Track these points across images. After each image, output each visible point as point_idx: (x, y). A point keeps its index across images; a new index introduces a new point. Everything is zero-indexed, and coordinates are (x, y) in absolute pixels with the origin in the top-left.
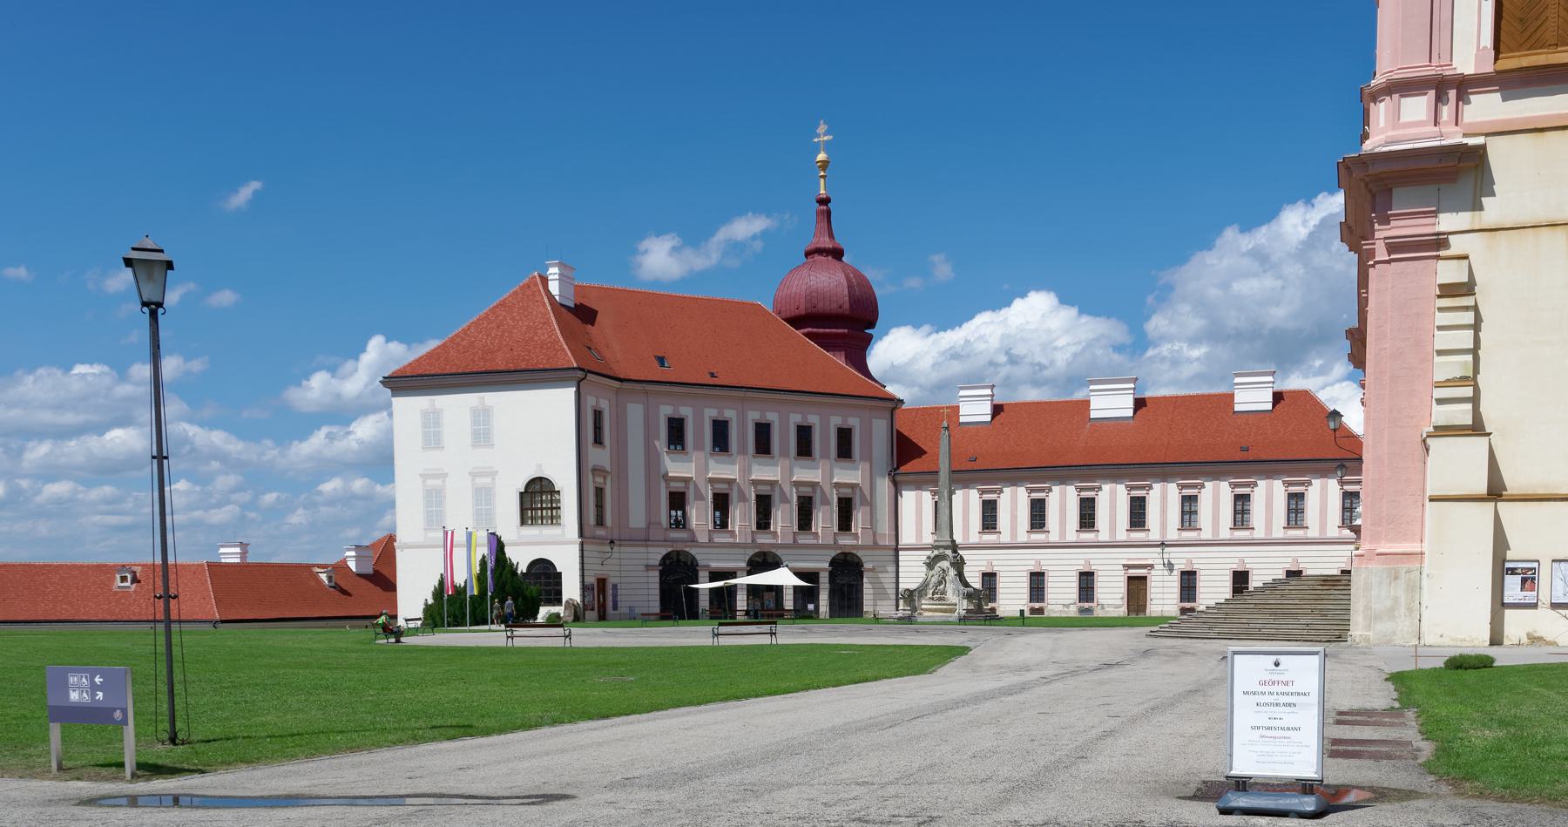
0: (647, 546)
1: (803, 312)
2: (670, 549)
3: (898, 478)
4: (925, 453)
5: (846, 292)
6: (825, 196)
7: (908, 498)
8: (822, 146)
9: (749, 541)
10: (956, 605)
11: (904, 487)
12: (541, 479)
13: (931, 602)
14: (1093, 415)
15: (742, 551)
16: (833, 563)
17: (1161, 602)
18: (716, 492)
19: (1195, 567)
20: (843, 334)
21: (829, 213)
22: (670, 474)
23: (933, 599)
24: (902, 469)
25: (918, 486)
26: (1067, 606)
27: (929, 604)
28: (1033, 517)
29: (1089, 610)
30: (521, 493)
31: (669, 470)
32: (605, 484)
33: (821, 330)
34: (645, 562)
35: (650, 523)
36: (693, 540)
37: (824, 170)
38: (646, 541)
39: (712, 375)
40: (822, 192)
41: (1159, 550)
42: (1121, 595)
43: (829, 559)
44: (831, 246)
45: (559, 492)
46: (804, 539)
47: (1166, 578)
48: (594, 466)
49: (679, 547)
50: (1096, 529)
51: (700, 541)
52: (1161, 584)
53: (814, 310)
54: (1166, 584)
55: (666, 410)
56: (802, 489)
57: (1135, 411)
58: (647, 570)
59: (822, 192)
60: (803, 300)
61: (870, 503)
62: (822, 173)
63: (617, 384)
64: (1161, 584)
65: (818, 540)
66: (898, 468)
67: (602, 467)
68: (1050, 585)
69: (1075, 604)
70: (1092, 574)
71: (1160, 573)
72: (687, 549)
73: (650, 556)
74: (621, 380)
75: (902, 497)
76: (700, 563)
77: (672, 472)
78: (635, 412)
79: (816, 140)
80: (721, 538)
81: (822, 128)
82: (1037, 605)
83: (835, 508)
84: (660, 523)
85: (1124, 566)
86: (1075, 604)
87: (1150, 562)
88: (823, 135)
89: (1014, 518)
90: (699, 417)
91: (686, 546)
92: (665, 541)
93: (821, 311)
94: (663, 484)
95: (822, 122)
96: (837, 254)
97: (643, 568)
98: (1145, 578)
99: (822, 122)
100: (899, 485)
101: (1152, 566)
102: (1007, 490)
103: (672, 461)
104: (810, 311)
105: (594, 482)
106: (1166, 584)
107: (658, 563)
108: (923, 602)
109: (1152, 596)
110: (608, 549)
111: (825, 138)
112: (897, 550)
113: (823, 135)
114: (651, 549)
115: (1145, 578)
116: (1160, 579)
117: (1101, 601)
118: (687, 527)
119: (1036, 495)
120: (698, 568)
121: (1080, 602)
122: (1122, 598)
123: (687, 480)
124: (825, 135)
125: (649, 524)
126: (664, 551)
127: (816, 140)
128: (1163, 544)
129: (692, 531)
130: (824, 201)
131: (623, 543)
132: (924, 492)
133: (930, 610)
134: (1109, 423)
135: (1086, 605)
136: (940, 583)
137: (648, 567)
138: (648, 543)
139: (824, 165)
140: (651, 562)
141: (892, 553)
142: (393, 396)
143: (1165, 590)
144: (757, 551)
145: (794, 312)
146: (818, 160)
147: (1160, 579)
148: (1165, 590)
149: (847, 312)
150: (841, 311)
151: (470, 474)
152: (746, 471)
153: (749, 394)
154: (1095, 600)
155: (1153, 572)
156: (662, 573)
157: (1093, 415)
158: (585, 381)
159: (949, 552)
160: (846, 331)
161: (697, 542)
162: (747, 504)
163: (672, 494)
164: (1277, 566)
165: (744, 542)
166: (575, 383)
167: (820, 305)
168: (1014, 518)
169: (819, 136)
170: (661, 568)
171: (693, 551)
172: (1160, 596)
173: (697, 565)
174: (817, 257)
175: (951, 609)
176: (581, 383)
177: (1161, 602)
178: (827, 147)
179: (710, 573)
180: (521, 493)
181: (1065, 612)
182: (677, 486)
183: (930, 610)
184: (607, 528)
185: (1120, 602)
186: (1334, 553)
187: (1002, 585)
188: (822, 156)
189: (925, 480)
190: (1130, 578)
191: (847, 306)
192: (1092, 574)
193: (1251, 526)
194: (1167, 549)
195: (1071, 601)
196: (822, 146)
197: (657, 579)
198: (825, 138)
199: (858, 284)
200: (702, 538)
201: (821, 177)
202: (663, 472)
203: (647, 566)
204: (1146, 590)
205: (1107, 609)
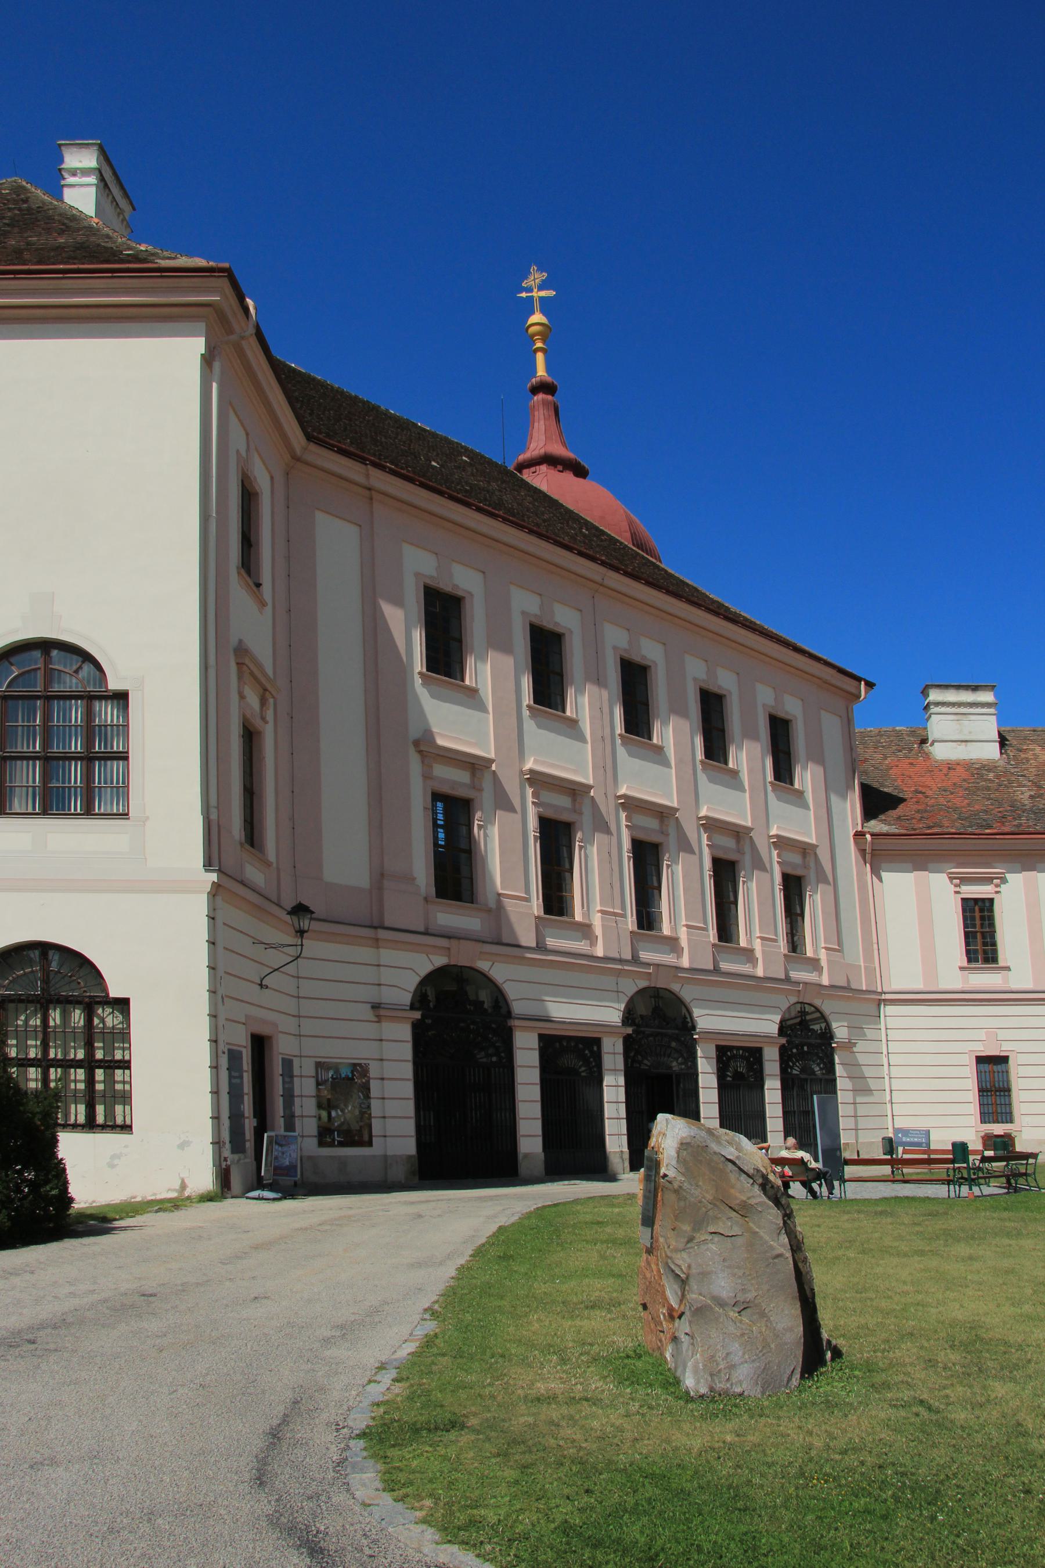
0: (376, 943)
2: (440, 961)
8: (537, 305)
9: (627, 955)
31: (435, 730)
34: (370, 994)
37: (544, 341)
49: (464, 956)
58: (379, 1019)
59: (541, 371)
62: (539, 345)
72: (483, 965)
73: (387, 976)
76: (517, 1008)
77: (442, 736)
79: (524, 295)
81: (536, 277)
92: (426, 933)
107: (407, 999)
111: (543, 294)
114: (387, 955)
123: (475, 766)
124: (541, 288)
125: (380, 877)
126: (425, 964)
127: (524, 295)
138: (382, 934)
140: (389, 996)
152: (610, 770)
156: (418, 1030)
169: (529, 290)
170: (417, 1015)
171: (500, 972)
173: (509, 1014)
179: (542, 1037)
182: (453, 778)
196: (537, 305)
197: (406, 1051)
198: (543, 294)
200: (527, 937)
202: (414, 733)
203: (376, 1007)
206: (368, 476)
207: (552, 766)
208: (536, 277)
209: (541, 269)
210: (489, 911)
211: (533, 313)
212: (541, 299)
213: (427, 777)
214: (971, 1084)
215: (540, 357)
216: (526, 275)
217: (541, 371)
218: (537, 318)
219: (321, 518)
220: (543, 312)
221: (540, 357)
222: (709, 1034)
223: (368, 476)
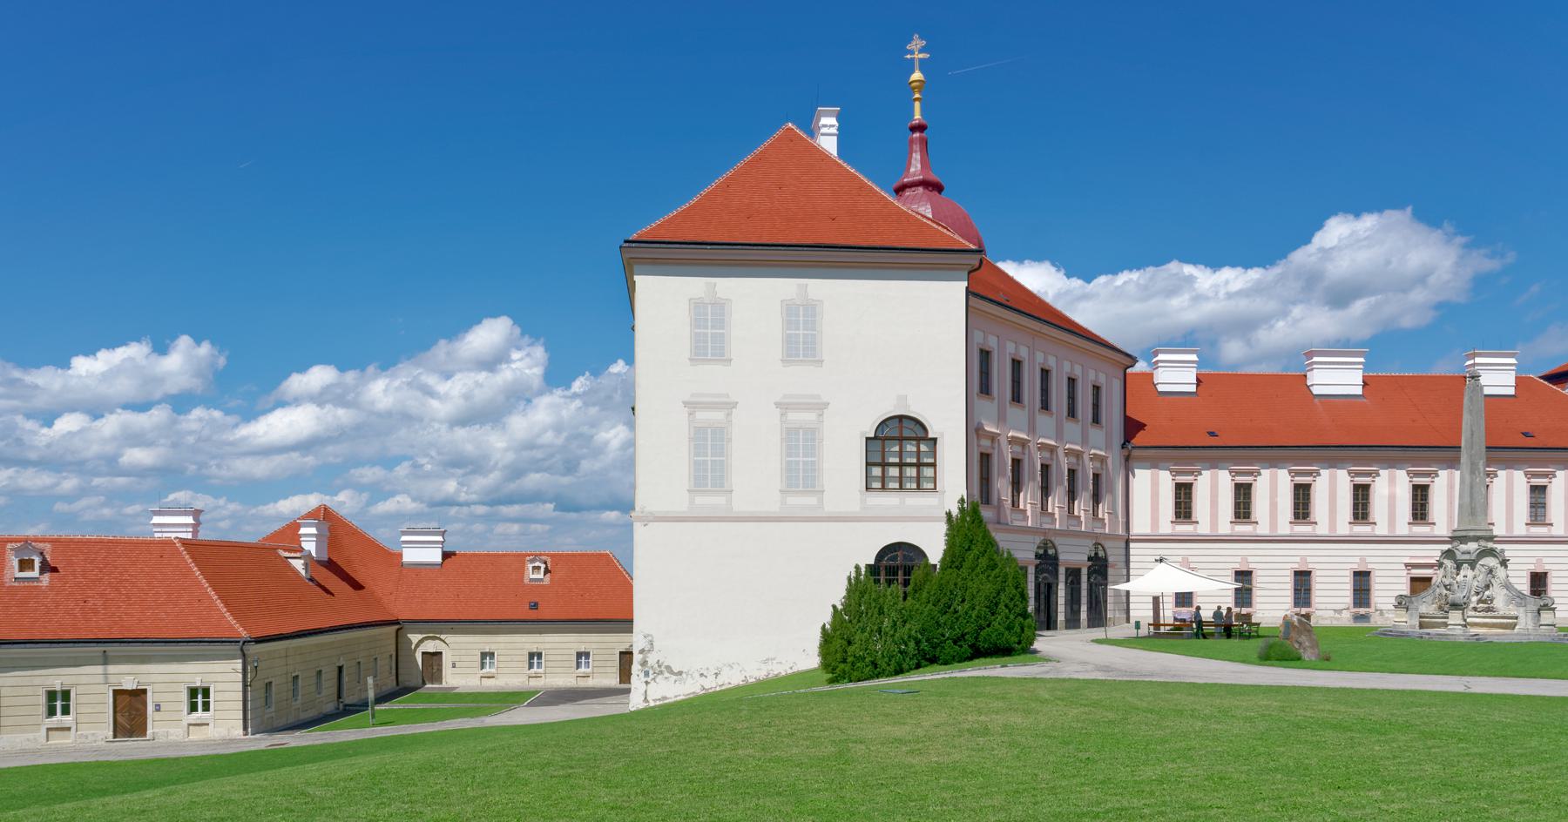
4: (1145, 425)
6: (917, 122)
7: (1142, 479)
8: (917, 64)
10: (1517, 618)
12: (901, 418)
18: (1015, 457)
19: (1251, 566)
23: (1475, 609)
24: (1136, 441)
25: (1154, 464)
26: (1339, 611)
29: (1365, 617)
30: (867, 439)
37: (920, 92)
45: (935, 440)
50: (1194, 519)
59: (917, 116)
62: (917, 96)
69: (1348, 609)
70: (1367, 574)
79: (909, 56)
81: (916, 44)
82: (1304, 611)
85: (1407, 565)
86: (1348, 609)
88: (916, 49)
89: (1274, 506)
95: (916, 36)
99: (916, 36)
100: (1131, 463)
102: (1266, 473)
111: (921, 56)
112: (1127, 542)
113: (916, 49)
117: (1380, 606)
124: (921, 51)
127: (909, 56)
130: (920, 128)
132: (1161, 472)
135: (1362, 611)
141: (1123, 545)
151: (778, 405)
154: (1373, 605)
163: (982, 454)
164: (1351, 560)
168: (1274, 506)
169: (912, 52)
175: (1511, 624)
178: (924, 67)
180: (867, 439)
181: (1338, 619)
186: (1267, 552)
189: (1161, 455)
190: (1413, 580)
193: (1547, 522)
195: (1343, 606)
196: (917, 64)
198: (921, 56)
205: (1387, 615)
208: (916, 44)
209: (921, 38)
211: (913, 72)
212: (920, 59)
213: (979, 446)
215: (917, 105)
216: (910, 40)
217: (917, 116)
218: (917, 76)
220: (921, 70)
221: (917, 105)
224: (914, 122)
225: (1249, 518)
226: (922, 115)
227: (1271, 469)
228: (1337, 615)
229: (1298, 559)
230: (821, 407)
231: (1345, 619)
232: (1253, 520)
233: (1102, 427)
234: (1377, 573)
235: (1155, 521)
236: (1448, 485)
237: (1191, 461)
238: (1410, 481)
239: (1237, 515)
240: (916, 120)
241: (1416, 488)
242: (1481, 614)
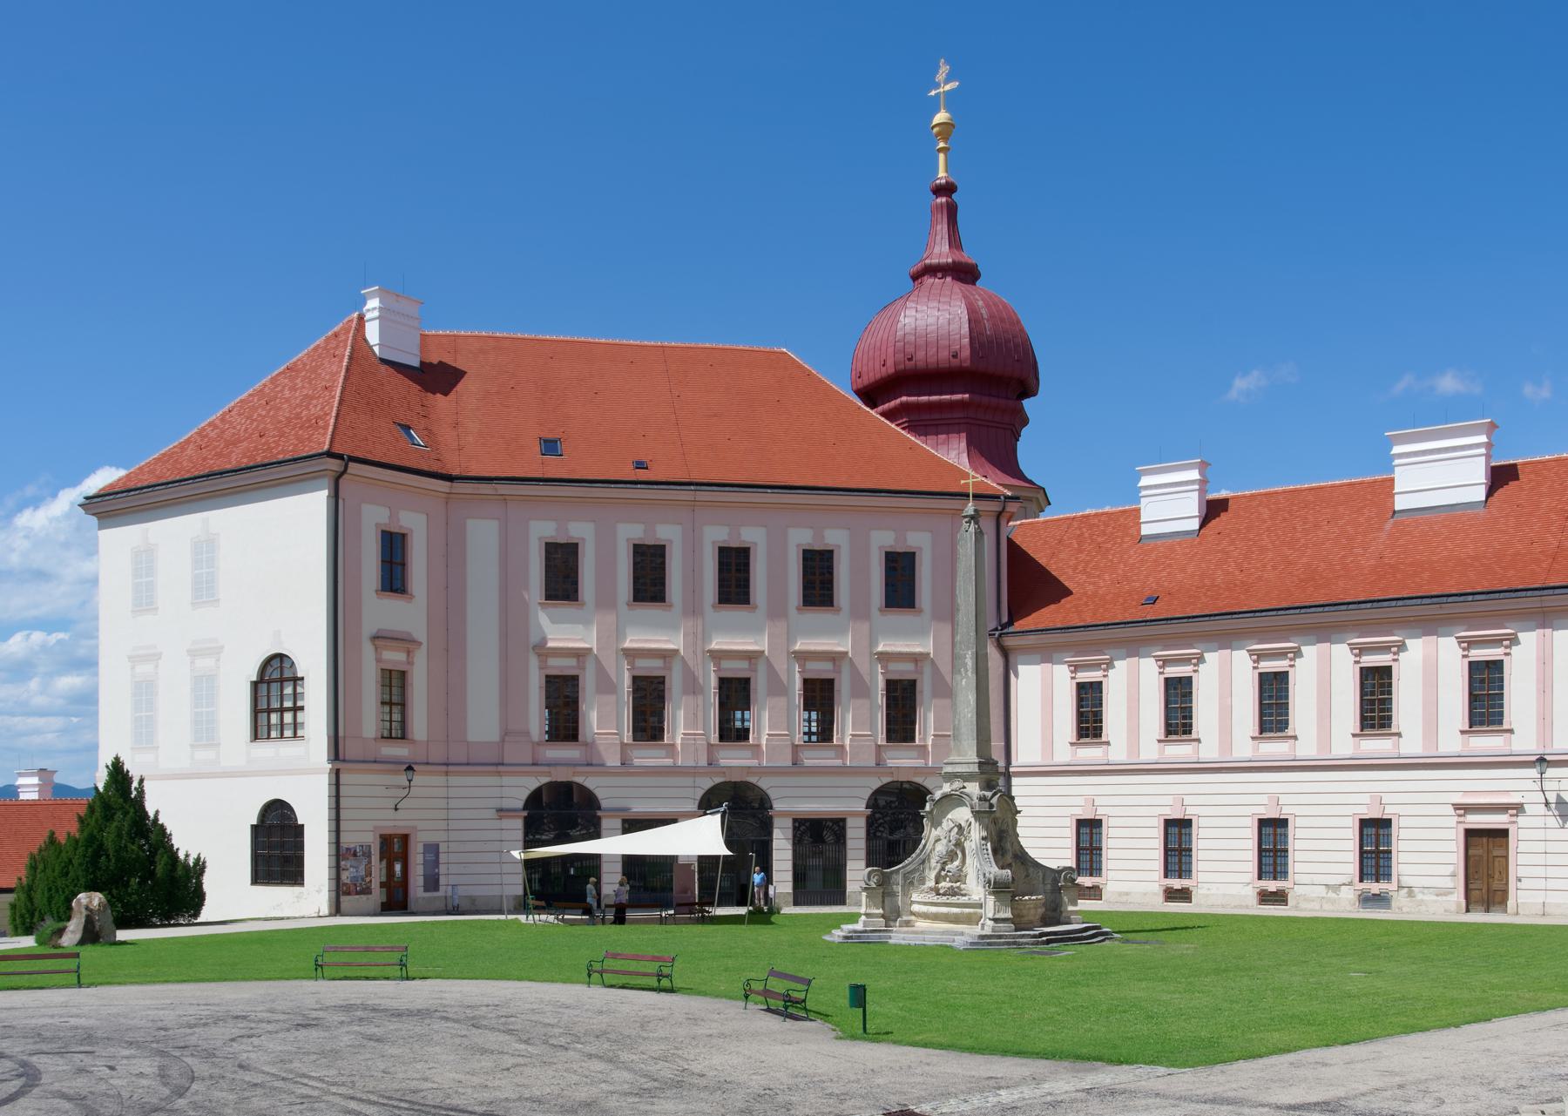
0: (499, 774)
1: (891, 371)
2: (545, 780)
3: (1009, 642)
4: (1068, 592)
5: (965, 329)
6: (943, 181)
9: (703, 762)
11: (1020, 658)
12: (281, 657)
13: (936, 899)
14: (1400, 503)
15: (688, 781)
16: (873, 802)
17: (1541, 884)
20: (961, 403)
21: (952, 211)
22: (550, 644)
24: (1019, 625)
25: (1046, 655)
27: (925, 904)
28: (1263, 709)
32: (410, 663)
33: (924, 398)
35: (506, 734)
36: (592, 764)
37: (946, 139)
38: (498, 767)
39: (640, 465)
40: (942, 175)
41: (1533, 773)
42: (1450, 869)
43: (867, 794)
44: (950, 260)
45: (302, 679)
46: (817, 757)
47: (1551, 834)
48: (379, 630)
49: (562, 775)
51: (608, 764)
52: (1540, 847)
53: (910, 365)
54: (1551, 847)
55: (543, 530)
56: (726, 664)
57: (1490, 492)
59: (942, 174)
60: (891, 350)
61: (945, 691)
62: (942, 145)
63: (443, 486)
64: (1540, 847)
65: (926, 759)
66: (1010, 623)
67: (409, 634)
68: (1298, 845)
69: (1350, 884)
70: (1386, 823)
71: (1539, 822)
74: (449, 478)
75: (1017, 676)
78: (483, 534)
79: (933, 93)
80: (648, 756)
81: (944, 70)
83: (880, 699)
84: (527, 733)
86: (1350, 884)
87: (1514, 799)
89: (1226, 713)
90: (693, 547)
91: (575, 774)
93: (921, 365)
94: (534, 662)
96: (965, 273)
97: (492, 814)
98: (1503, 833)
101: (1519, 808)
102: (1212, 658)
103: (553, 622)
104: (902, 367)
105: (378, 660)
106: (1551, 847)
107: (520, 804)
108: (915, 897)
109: (1522, 872)
110: (402, 779)
111: (948, 87)
115: (1503, 833)
116: (1540, 834)
117: (1406, 881)
118: (580, 737)
119: (1270, 666)
120: (599, 813)
121: (1361, 880)
122: (1454, 875)
123: (580, 654)
124: (947, 82)
126: (533, 783)
127: (933, 93)
128: (1542, 760)
129: (590, 746)
130: (947, 189)
131: (451, 768)
133: (925, 916)
134: (1418, 516)
135: (1375, 887)
136: (951, 856)
137: (502, 812)
138: (501, 768)
139: (946, 130)
140: (507, 804)
142: (99, 529)
143: (1551, 859)
144: (718, 780)
145: (874, 373)
146: (934, 123)
147: (1540, 834)
148: (1551, 859)
149: (967, 364)
150: (955, 362)
153: (705, 495)
154: (1394, 878)
155: (1521, 820)
157: (1400, 503)
158: (345, 476)
159: (974, 789)
160: (967, 396)
161: (603, 765)
162: (700, 698)
165: (692, 763)
166: (326, 481)
167: (920, 355)
168: (1226, 713)
169: (937, 86)
171: (591, 783)
172: (1540, 871)
174: (928, 281)
176: (341, 481)
177: (1541, 884)
181: (1333, 902)
183: (925, 916)
184: (413, 742)
185: (1448, 883)
187: (1203, 844)
188: (941, 117)
190: (1470, 833)
191: (966, 353)
192: (1386, 823)
194: (1551, 772)
199: (991, 317)
200: (613, 760)
201: (940, 150)
202: (534, 639)
203: (500, 810)
204: (1506, 857)
206: (496, 489)
207: (646, 641)
210: (586, 744)
211: (938, 111)
214: (1251, 844)
217: (942, 174)
219: (470, 523)
221: (942, 156)
222: (784, 814)
223: (496, 489)
224: (938, 182)
225: (1500, 723)
226: (947, 171)
227: (1424, 638)
228: (1331, 895)
229: (1080, 801)
230: (216, 651)
231: (1345, 904)
232: (1505, 727)
233: (921, 611)
234: (1404, 822)
235: (1048, 742)
236: (1538, 659)
237: (1097, 647)
238: (1464, 656)
239: (1264, 727)
240: (941, 178)
241: (1474, 667)
242: (944, 899)
